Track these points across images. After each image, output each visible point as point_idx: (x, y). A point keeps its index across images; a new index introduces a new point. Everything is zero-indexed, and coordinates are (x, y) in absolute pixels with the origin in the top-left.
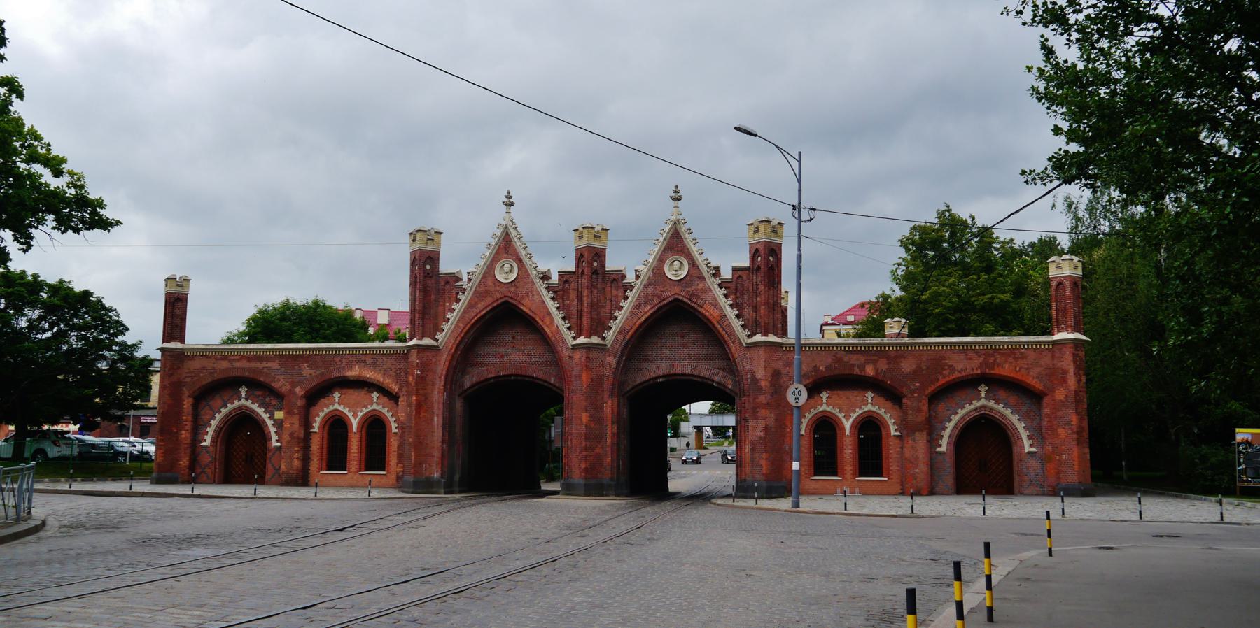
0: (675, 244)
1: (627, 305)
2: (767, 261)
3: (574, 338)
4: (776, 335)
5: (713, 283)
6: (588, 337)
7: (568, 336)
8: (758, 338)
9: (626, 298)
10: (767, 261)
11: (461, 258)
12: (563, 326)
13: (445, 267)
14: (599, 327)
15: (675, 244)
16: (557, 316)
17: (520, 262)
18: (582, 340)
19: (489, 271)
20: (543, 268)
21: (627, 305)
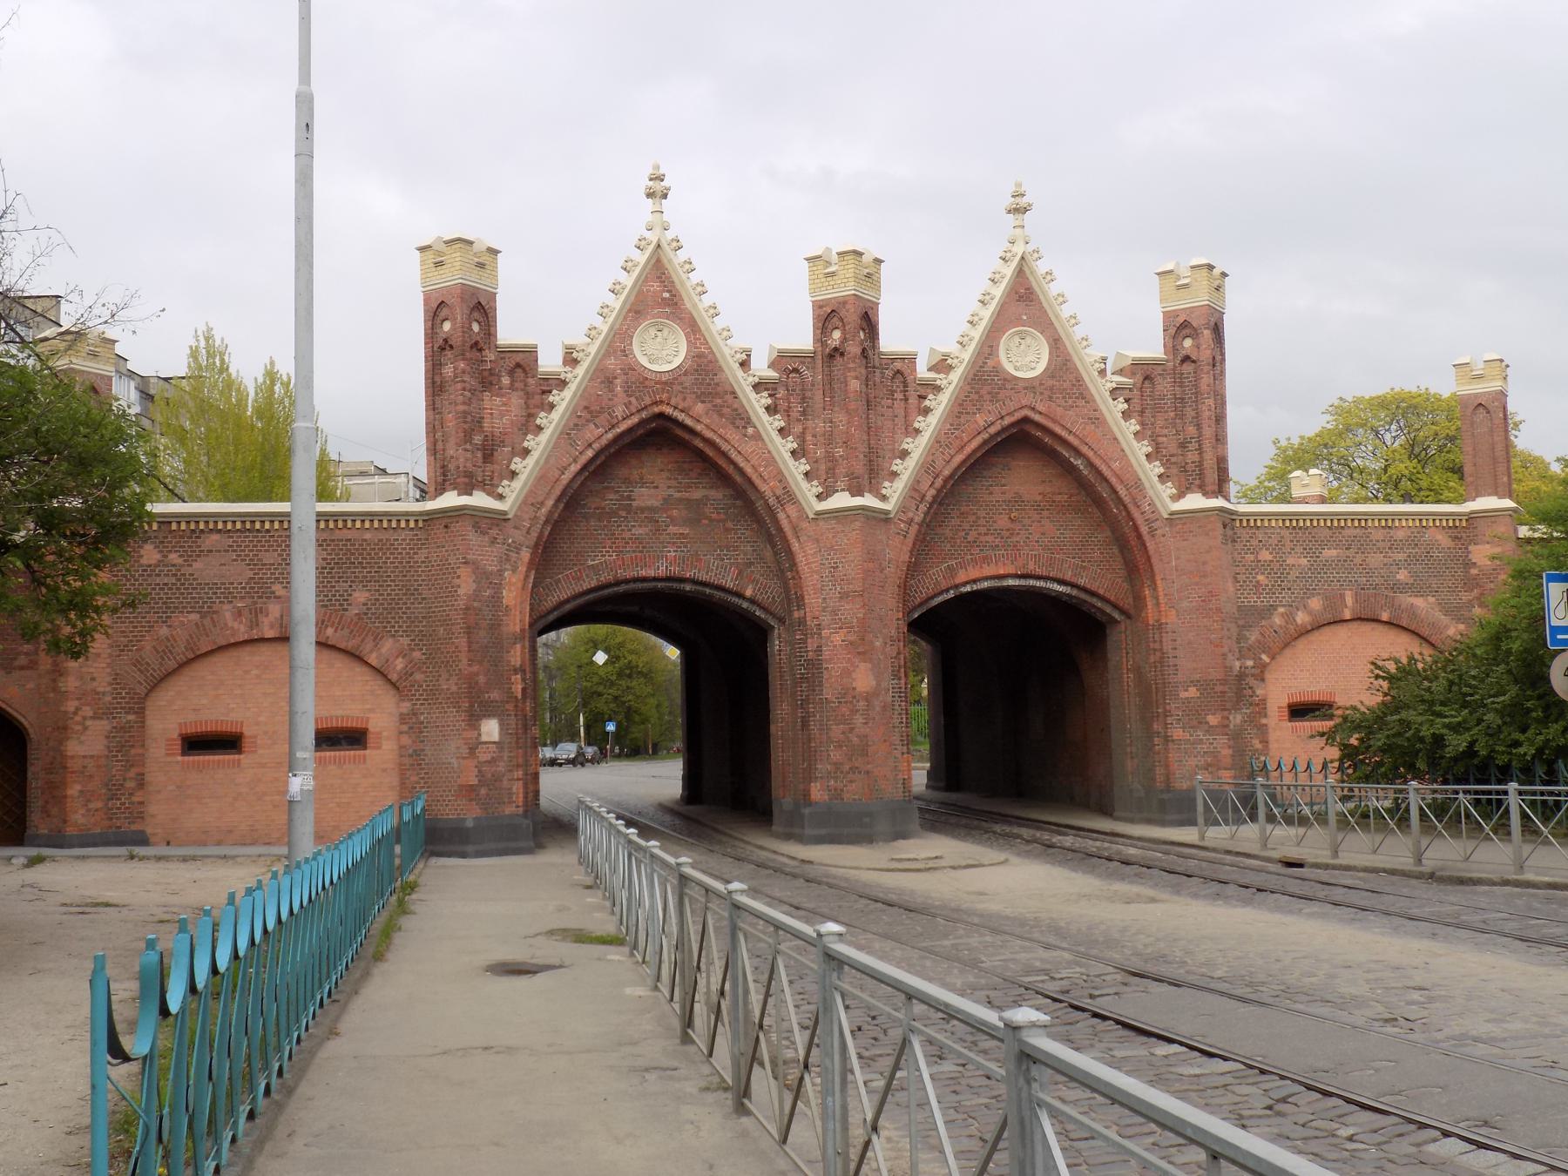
0: (1023, 300)
1: (929, 425)
2: (1197, 339)
3: (819, 497)
4: (1206, 494)
5: (1100, 389)
6: (857, 491)
7: (807, 492)
8: (1194, 501)
9: (926, 411)
10: (1197, 339)
11: (553, 314)
12: (795, 470)
13: (509, 331)
14: (871, 476)
15: (1023, 300)
16: (783, 448)
17: (693, 328)
18: (841, 500)
19: (618, 342)
20: (738, 342)
21: (929, 425)
